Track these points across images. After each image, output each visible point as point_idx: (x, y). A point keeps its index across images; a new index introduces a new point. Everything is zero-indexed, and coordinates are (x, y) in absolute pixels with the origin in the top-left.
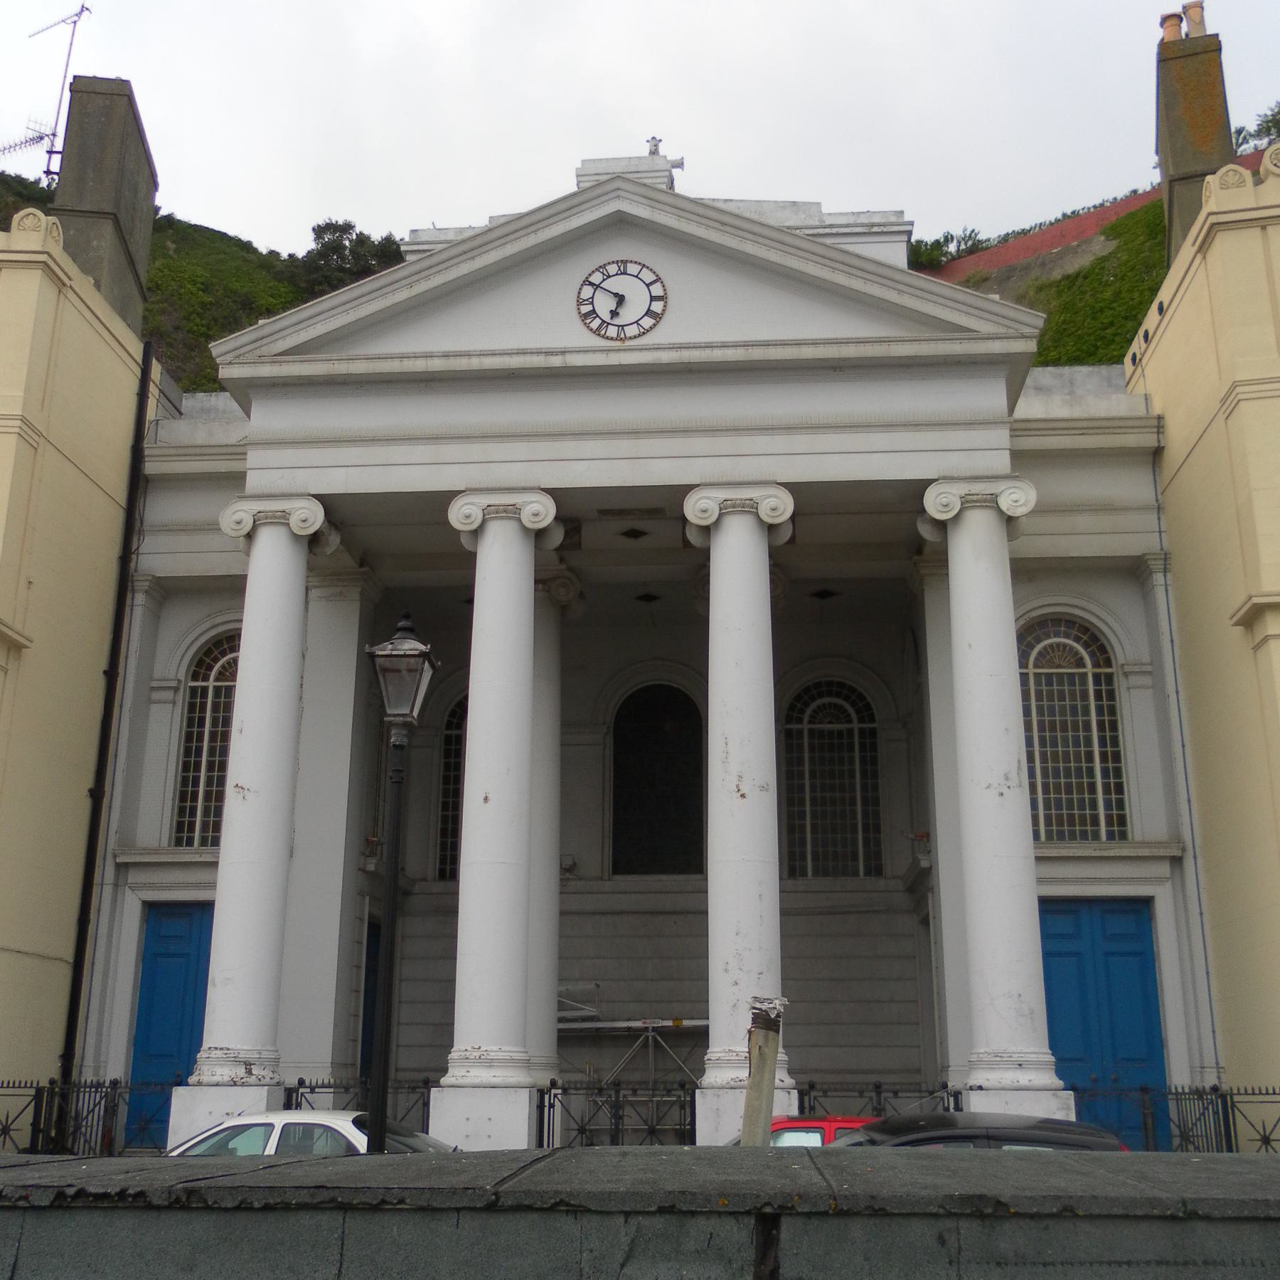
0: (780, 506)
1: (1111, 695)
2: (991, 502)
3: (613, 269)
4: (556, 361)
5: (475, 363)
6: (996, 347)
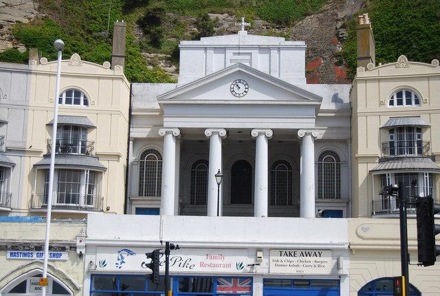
0: (270, 134)
1: (339, 168)
2: (311, 134)
3: (241, 95)
4: (227, 102)
5: (210, 102)
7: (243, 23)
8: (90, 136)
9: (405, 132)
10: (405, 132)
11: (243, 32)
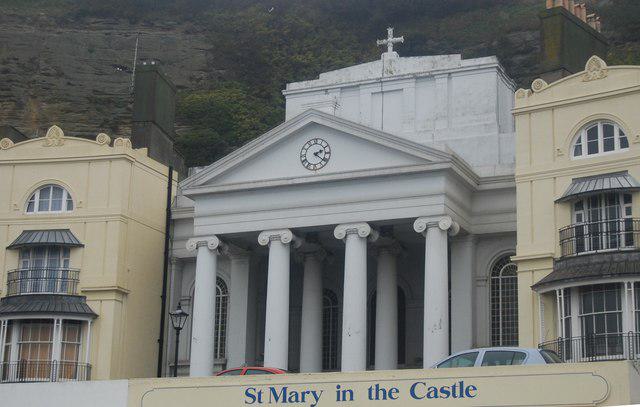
2: (436, 225)
6: (437, 167)
7: (390, 39)
8: (75, 260)
9: (603, 208)
10: (603, 208)
11: (390, 55)
